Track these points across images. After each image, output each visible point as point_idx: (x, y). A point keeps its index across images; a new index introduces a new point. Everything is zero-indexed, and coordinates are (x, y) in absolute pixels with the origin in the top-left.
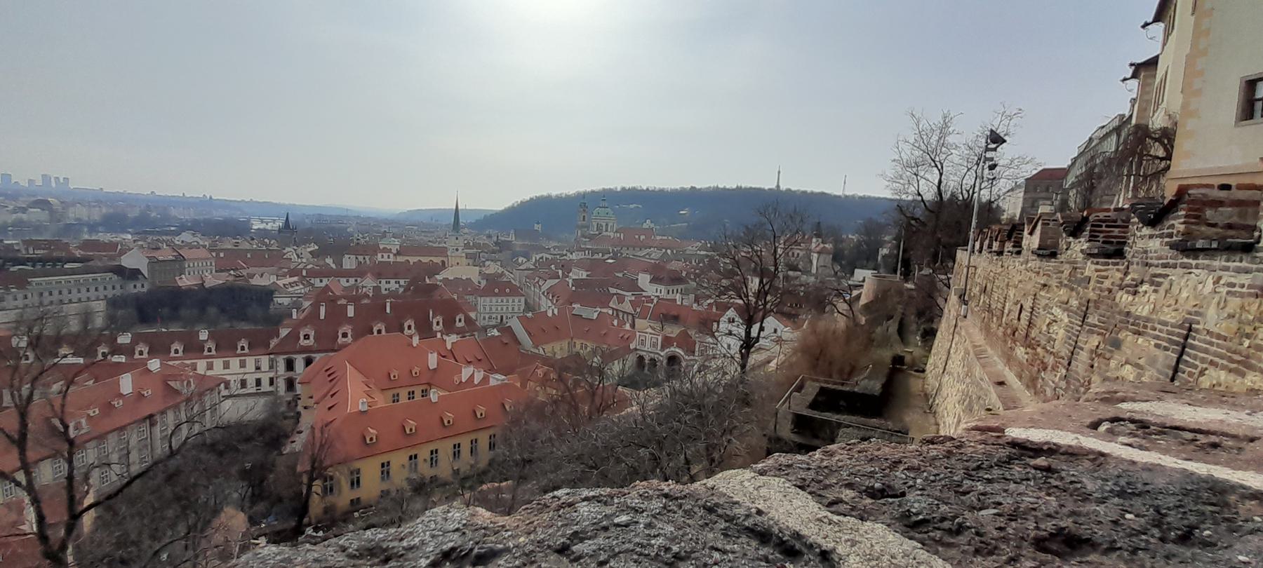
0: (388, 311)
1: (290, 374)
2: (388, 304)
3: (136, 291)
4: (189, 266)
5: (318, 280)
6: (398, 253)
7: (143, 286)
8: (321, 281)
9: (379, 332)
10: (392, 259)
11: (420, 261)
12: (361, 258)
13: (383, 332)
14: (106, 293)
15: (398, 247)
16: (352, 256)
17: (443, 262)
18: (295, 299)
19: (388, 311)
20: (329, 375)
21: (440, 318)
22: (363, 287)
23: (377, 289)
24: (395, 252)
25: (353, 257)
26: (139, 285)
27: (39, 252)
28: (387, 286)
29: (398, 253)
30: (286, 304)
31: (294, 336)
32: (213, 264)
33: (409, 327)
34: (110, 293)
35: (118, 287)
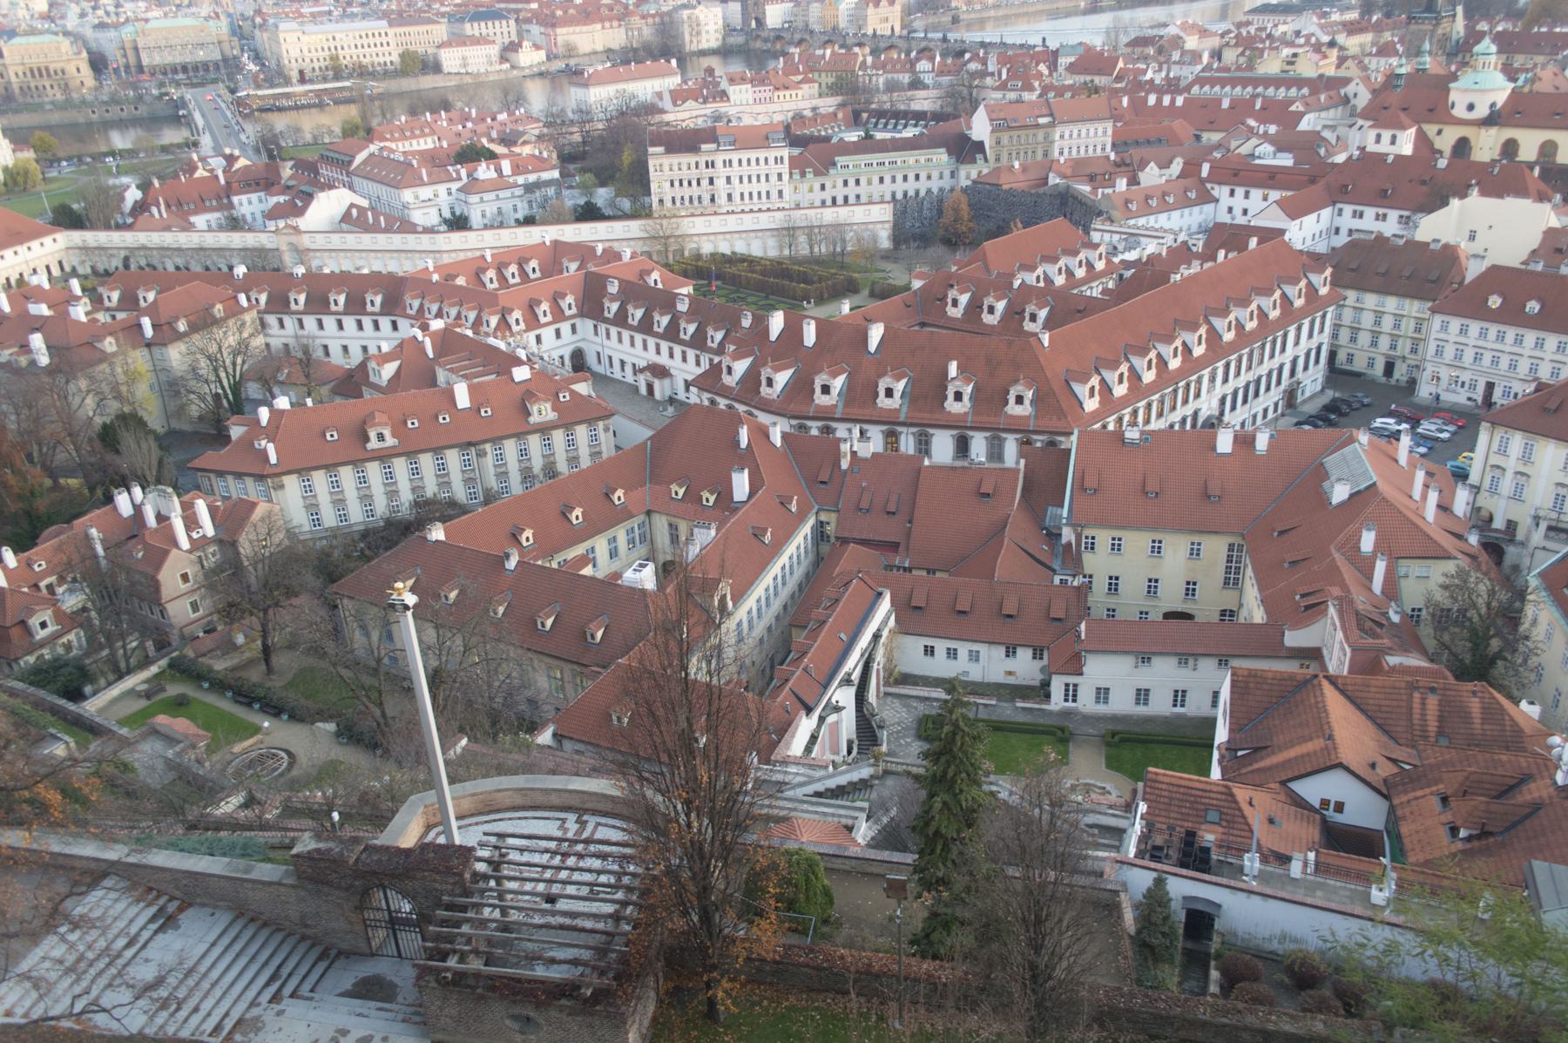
4: (1062, 137)
5: (1226, 190)
8: (1232, 193)
32: (1110, 132)
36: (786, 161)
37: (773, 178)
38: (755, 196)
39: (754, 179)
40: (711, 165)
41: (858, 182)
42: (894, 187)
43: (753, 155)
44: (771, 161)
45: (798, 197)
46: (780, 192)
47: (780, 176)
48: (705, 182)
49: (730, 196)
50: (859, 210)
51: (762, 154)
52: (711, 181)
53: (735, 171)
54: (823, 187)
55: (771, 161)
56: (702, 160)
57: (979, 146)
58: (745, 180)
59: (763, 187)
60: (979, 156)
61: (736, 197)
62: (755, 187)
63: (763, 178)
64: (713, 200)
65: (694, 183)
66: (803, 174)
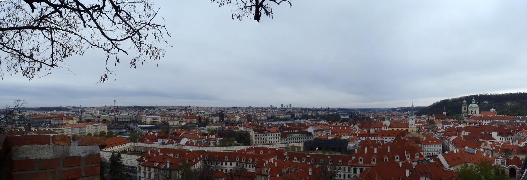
0: (389, 151)
1: (355, 174)
2: (389, 149)
3: (310, 140)
5: (362, 138)
6: (390, 127)
7: (312, 138)
8: (363, 138)
9: (386, 160)
10: (387, 129)
11: (398, 129)
12: (376, 129)
13: (387, 160)
14: (303, 140)
15: (390, 124)
16: (373, 128)
17: (407, 130)
18: (355, 145)
19: (389, 151)
20: (369, 177)
21: (409, 155)
22: (378, 140)
23: (382, 141)
24: (388, 126)
25: (373, 128)
26: (311, 138)
27: (289, 127)
28: (386, 140)
29: (390, 127)
30: (352, 146)
31: (356, 161)
33: (397, 158)
34: (304, 140)
35: (306, 138)
36: (280, 135)
37: (278, 138)
38: (274, 141)
39: (274, 138)
42: (303, 140)
43: (274, 134)
44: (277, 135)
45: (282, 142)
46: (279, 141)
47: (279, 138)
48: (265, 139)
49: (269, 142)
50: (298, 143)
51: (276, 134)
52: (266, 139)
54: (286, 140)
55: (277, 135)
56: (265, 135)
57: (311, 133)
58: (272, 138)
59: (276, 140)
60: (311, 135)
64: (266, 142)
65: (263, 139)
66: (283, 138)
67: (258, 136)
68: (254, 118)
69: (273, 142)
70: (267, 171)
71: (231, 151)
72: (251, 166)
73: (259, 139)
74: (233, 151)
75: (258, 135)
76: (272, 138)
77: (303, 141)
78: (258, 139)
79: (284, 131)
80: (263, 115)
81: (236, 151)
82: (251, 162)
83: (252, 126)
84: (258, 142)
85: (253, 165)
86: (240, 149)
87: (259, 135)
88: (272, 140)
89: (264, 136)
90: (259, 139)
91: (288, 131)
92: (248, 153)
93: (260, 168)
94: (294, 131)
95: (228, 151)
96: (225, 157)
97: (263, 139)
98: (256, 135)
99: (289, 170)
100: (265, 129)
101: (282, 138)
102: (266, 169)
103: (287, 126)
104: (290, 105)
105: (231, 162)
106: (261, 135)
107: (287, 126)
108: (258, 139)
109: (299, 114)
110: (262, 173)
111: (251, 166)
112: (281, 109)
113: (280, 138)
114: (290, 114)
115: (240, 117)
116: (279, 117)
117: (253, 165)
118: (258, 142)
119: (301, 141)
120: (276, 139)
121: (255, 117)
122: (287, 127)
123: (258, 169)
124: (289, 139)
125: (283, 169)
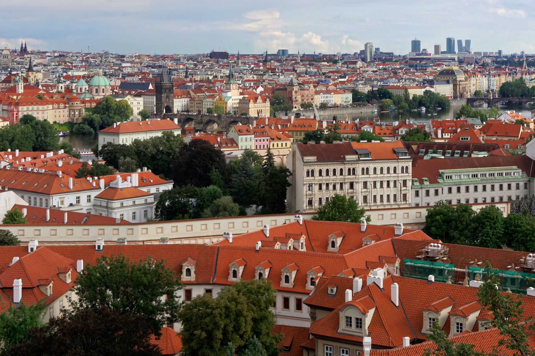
27: (447, 136)
34: (514, 193)
35: (522, 184)
38: (385, 198)
39: (385, 184)
40: (352, 172)
41: (459, 190)
43: (385, 166)
44: (399, 170)
45: (418, 200)
47: (405, 182)
48: (347, 186)
51: (392, 165)
52: (352, 186)
53: (371, 178)
55: (399, 170)
56: (346, 168)
58: (378, 185)
59: (392, 191)
61: (370, 199)
62: (386, 191)
63: (392, 184)
67: (317, 173)
68: (299, 98)
69: (382, 200)
70: (359, 323)
71: (207, 242)
72: (292, 303)
73: (324, 187)
74: (215, 240)
75: (317, 169)
76: (375, 183)
77: (510, 198)
78: (320, 188)
79: (426, 153)
80: (335, 85)
81: (231, 241)
82: (290, 285)
83: (293, 131)
84: (320, 199)
85: (299, 296)
86: (244, 231)
87: (324, 169)
88: (378, 192)
89: (345, 172)
90: (324, 187)
91: (444, 154)
92: (277, 246)
93: (330, 310)
94: (470, 156)
95: (193, 242)
96: (181, 267)
97: (341, 188)
98: (310, 169)
99: (453, 319)
100: (349, 145)
101: (417, 184)
102: (353, 314)
103: (439, 132)
104: (450, 42)
105: (208, 287)
106: (331, 168)
107: (436, 134)
108: (320, 188)
109: (489, 81)
110: (340, 331)
111: (292, 303)
112: (411, 59)
113: (409, 184)
114: (448, 82)
115: (241, 94)
116: (401, 93)
117: (299, 296)
118: (320, 199)
119: (501, 199)
120: (395, 186)
121: (303, 96)
122: (440, 136)
123: (320, 315)
124: (446, 189)
125: (425, 314)
